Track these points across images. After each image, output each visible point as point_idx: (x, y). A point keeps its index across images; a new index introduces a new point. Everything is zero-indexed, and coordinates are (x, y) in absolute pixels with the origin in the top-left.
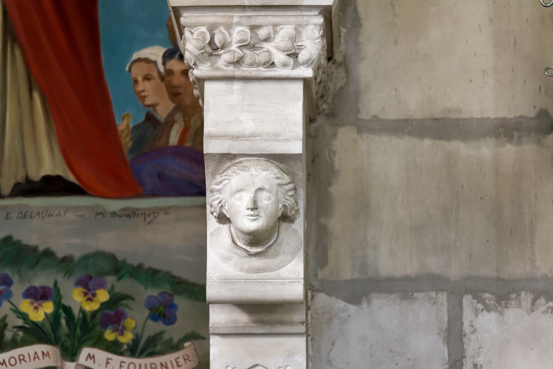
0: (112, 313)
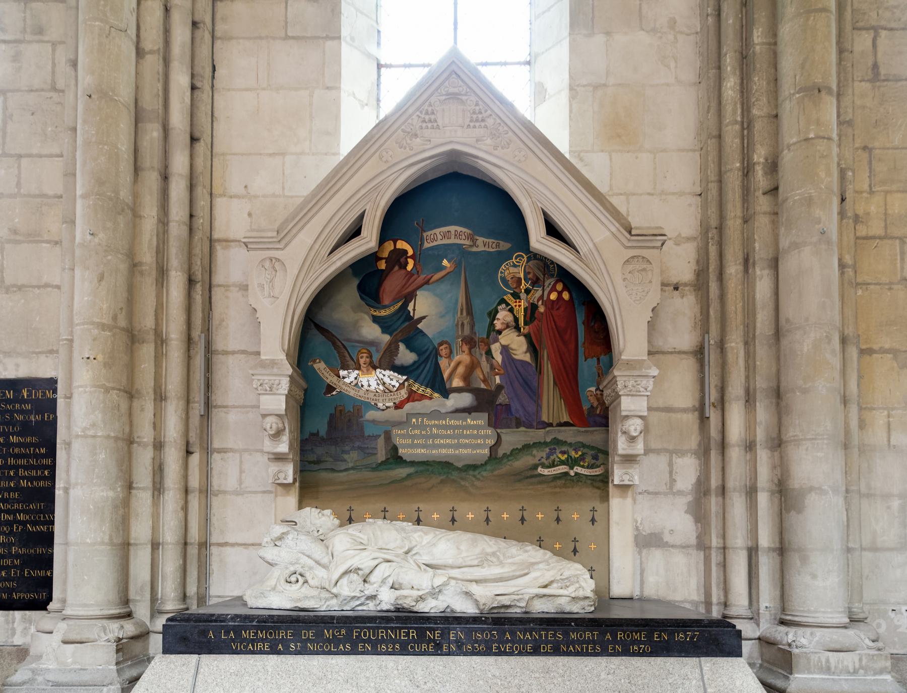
0: (582, 458)
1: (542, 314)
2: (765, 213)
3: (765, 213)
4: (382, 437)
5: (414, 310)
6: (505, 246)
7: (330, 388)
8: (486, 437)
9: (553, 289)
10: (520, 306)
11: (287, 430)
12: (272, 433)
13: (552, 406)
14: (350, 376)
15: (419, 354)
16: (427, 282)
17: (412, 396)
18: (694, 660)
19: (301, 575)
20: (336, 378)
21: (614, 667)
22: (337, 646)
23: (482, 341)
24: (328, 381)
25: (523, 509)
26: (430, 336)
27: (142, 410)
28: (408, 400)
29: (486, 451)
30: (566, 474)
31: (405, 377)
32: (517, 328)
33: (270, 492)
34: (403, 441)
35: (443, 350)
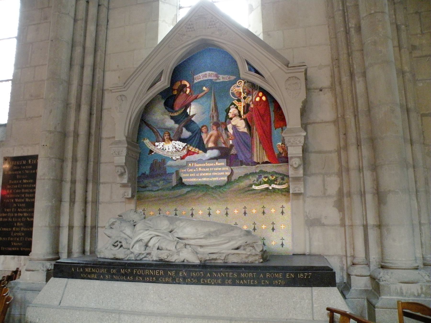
0: (276, 180)
1: (252, 108)
2: (357, 50)
3: (357, 50)
4: (175, 173)
5: (190, 111)
6: (233, 78)
7: (151, 151)
8: (226, 171)
9: (258, 96)
10: (241, 105)
11: (127, 173)
12: (119, 174)
13: (259, 153)
14: (160, 145)
15: (193, 133)
16: (196, 98)
17: (189, 153)
18: (309, 288)
19: (120, 242)
20: (154, 146)
21: (263, 292)
22: (126, 278)
23: (222, 123)
24: (150, 148)
25: (245, 208)
26: (198, 123)
27: (67, 166)
28: (187, 155)
29: (226, 178)
30: (267, 189)
31: (185, 144)
32: (240, 116)
33: (123, 202)
34: (184, 175)
35: (204, 130)
